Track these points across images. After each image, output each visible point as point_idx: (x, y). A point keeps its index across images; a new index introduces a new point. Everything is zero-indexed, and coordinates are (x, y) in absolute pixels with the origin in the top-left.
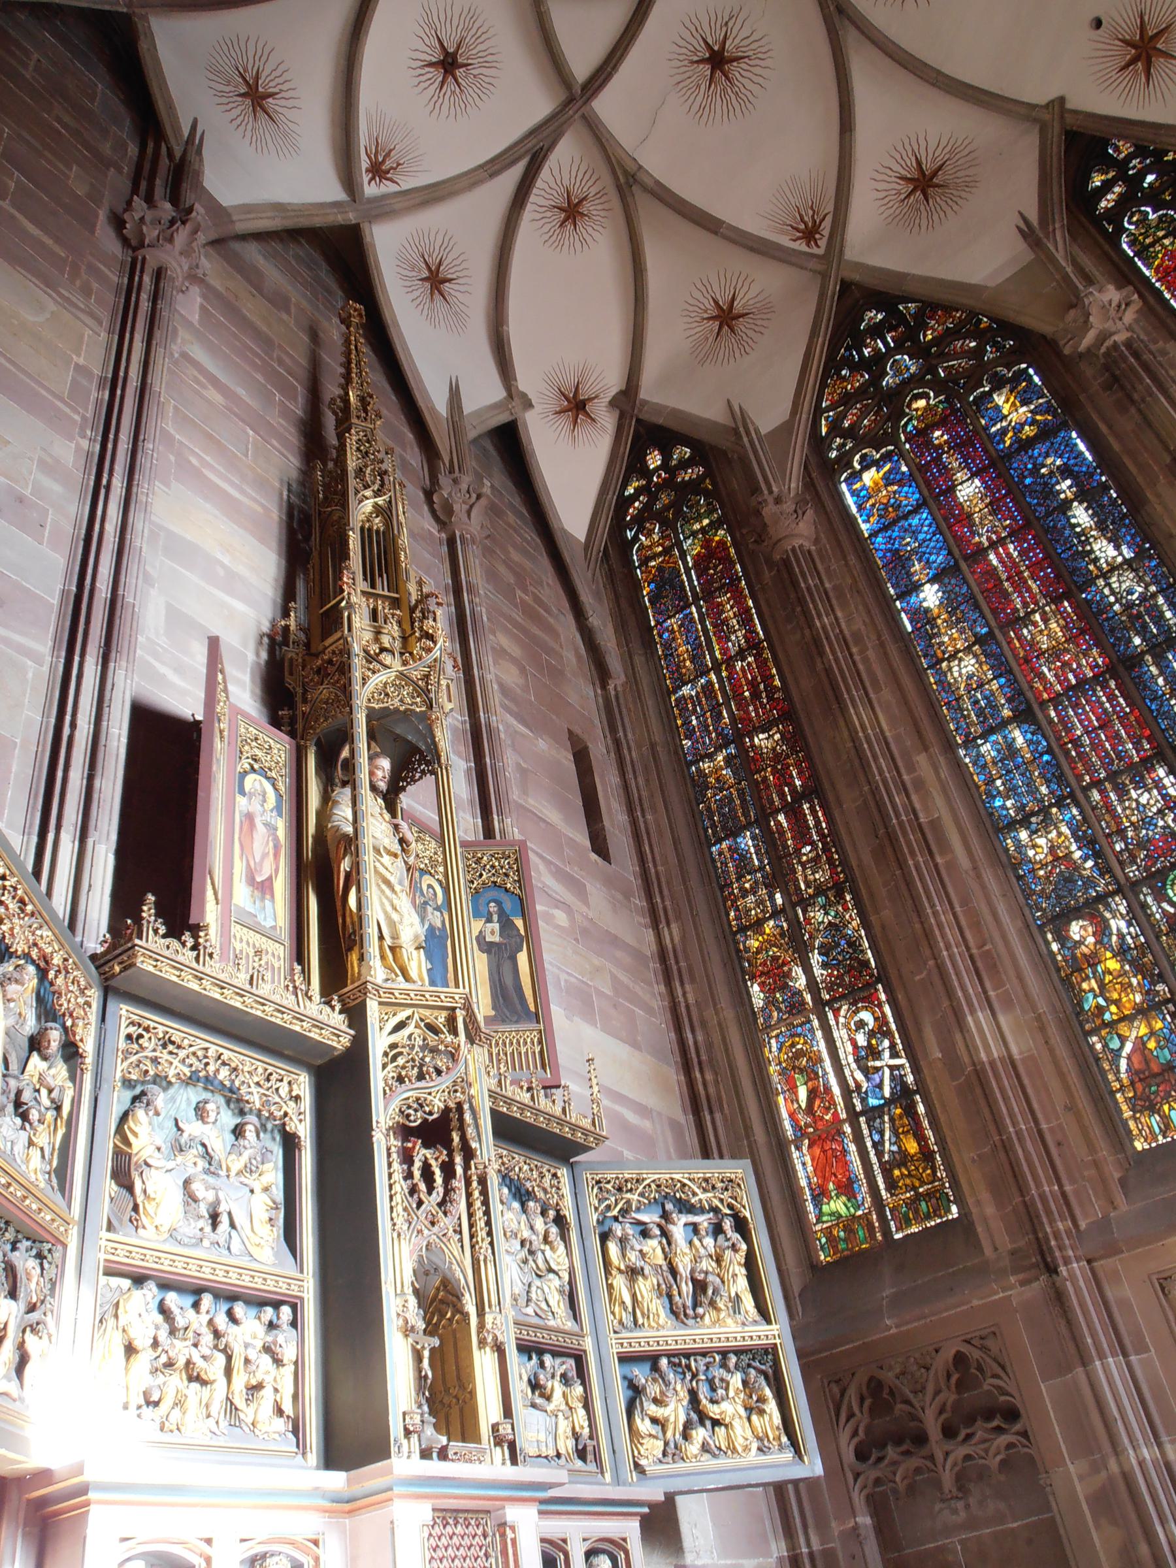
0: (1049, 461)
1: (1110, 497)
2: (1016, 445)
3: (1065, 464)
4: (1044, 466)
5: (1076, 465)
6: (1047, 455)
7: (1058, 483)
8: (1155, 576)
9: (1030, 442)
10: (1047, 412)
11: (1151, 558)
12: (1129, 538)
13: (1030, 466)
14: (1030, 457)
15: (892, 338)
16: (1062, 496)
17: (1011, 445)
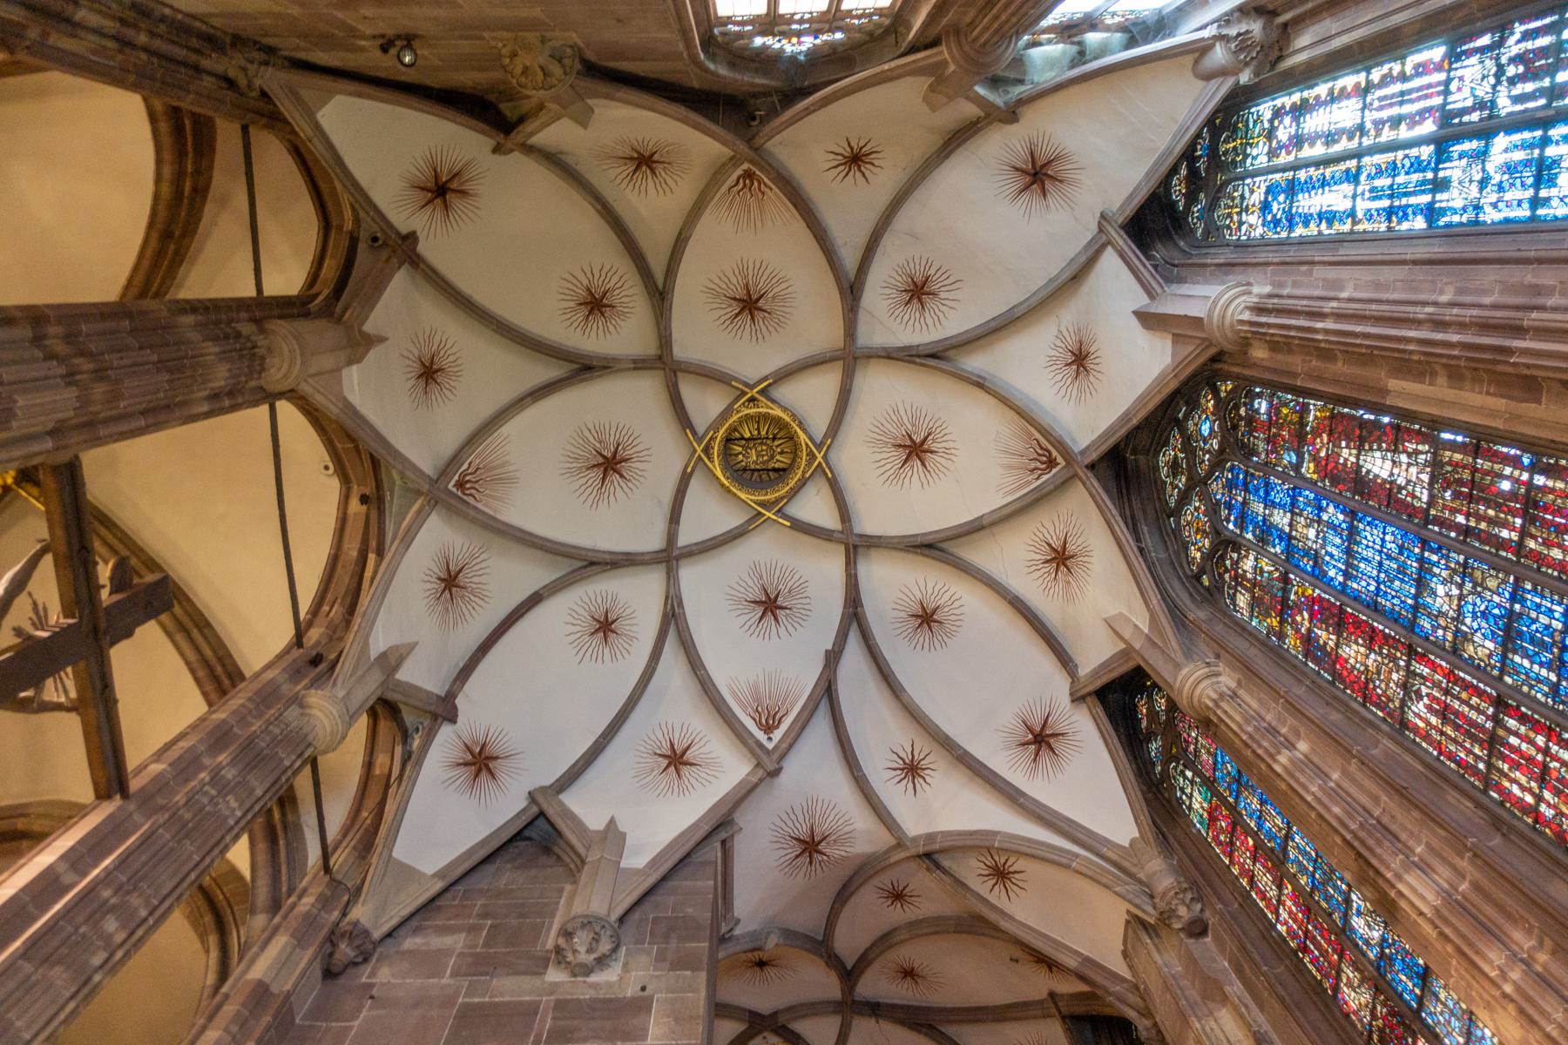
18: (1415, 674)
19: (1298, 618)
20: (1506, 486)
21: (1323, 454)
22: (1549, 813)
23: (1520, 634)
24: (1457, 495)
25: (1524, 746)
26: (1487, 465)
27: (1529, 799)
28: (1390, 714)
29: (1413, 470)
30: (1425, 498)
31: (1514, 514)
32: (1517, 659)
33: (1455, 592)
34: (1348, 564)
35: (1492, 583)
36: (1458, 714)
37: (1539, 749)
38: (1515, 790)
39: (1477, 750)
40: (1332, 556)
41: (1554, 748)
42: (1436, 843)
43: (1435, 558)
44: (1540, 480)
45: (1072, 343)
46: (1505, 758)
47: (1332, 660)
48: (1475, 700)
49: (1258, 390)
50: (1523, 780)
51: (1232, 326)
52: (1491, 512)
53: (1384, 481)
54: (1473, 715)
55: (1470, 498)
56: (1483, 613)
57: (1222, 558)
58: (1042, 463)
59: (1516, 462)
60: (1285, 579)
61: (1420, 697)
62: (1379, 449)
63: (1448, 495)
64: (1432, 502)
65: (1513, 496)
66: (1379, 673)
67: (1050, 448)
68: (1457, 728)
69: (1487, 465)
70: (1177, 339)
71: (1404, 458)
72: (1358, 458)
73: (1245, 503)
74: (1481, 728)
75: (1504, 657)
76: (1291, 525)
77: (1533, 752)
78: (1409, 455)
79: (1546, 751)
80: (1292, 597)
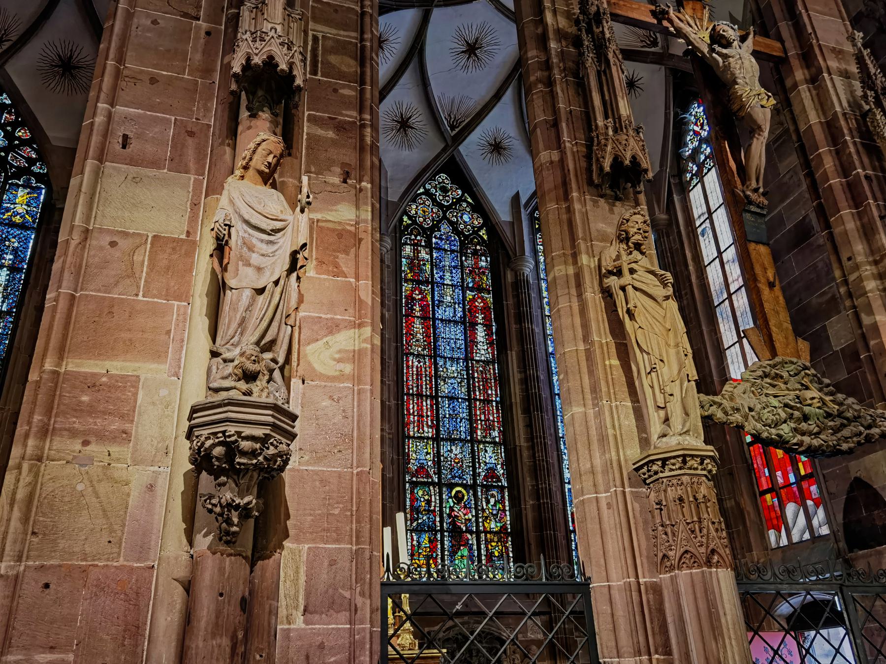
0: (13, 240)
1: (20, 277)
2: (7, 221)
3: (17, 247)
4: (9, 241)
5: (21, 251)
6: (14, 237)
7: (7, 254)
8: (6, 326)
9: (12, 225)
10: (32, 217)
11: (11, 316)
12: (11, 301)
13: (4, 236)
14: (8, 232)
15: (6, 117)
16: (3, 261)
17: (5, 219)
18: (425, 359)
19: (417, 292)
20: (490, 392)
21: (477, 304)
22: (412, 419)
23: (453, 402)
24: (481, 372)
25: (425, 408)
26: (493, 384)
27: (411, 411)
28: (407, 348)
29: (483, 352)
30: (477, 358)
31: (484, 396)
32: (447, 402)
33: (456, 375)
34: (446, 320)
35: (463, 390)
36: (421, 379)
37: (427, 413)
38: (411, 406)
39: (415, 389)
40: (445, 311)
41: (429, 418)
42: (392, 387)
43: (462, 364)
44: (494, 404)
45: (505, 143)
46: (418, 400)
47: (410, 314)
48: (428, 386)
49: (489, 259)
50: (415, 409)
51: (522, 269)
52: (481, 387)
53: (476, 338)
54: (424, 387)
55: (483, 378)
56: (454, 388)
57: (419, 234)
58: (453, 122)
59: (496, 395)
60: (427, 282)
61: (419, 362)
62: (486, 335)
63: (481, 369)
64: (478, 361)
65: (488, 395)
66: (417, 341)
67: (460, 127)
68: (417, 379)
69: (493, 384)
70: (512, 224)
71: (486, 347)
72: (480, 324)
73: (446, 251)
74: (422, 391)
75: (446, 397)
76: (447, 285)
77: (425, 411)
78: (487, 349)
79: (428, 416)
80: (423, 287)
